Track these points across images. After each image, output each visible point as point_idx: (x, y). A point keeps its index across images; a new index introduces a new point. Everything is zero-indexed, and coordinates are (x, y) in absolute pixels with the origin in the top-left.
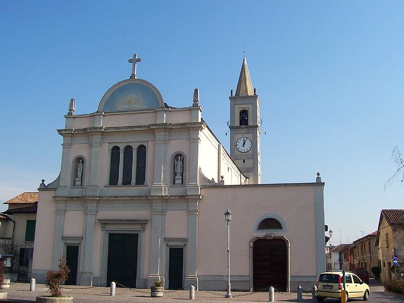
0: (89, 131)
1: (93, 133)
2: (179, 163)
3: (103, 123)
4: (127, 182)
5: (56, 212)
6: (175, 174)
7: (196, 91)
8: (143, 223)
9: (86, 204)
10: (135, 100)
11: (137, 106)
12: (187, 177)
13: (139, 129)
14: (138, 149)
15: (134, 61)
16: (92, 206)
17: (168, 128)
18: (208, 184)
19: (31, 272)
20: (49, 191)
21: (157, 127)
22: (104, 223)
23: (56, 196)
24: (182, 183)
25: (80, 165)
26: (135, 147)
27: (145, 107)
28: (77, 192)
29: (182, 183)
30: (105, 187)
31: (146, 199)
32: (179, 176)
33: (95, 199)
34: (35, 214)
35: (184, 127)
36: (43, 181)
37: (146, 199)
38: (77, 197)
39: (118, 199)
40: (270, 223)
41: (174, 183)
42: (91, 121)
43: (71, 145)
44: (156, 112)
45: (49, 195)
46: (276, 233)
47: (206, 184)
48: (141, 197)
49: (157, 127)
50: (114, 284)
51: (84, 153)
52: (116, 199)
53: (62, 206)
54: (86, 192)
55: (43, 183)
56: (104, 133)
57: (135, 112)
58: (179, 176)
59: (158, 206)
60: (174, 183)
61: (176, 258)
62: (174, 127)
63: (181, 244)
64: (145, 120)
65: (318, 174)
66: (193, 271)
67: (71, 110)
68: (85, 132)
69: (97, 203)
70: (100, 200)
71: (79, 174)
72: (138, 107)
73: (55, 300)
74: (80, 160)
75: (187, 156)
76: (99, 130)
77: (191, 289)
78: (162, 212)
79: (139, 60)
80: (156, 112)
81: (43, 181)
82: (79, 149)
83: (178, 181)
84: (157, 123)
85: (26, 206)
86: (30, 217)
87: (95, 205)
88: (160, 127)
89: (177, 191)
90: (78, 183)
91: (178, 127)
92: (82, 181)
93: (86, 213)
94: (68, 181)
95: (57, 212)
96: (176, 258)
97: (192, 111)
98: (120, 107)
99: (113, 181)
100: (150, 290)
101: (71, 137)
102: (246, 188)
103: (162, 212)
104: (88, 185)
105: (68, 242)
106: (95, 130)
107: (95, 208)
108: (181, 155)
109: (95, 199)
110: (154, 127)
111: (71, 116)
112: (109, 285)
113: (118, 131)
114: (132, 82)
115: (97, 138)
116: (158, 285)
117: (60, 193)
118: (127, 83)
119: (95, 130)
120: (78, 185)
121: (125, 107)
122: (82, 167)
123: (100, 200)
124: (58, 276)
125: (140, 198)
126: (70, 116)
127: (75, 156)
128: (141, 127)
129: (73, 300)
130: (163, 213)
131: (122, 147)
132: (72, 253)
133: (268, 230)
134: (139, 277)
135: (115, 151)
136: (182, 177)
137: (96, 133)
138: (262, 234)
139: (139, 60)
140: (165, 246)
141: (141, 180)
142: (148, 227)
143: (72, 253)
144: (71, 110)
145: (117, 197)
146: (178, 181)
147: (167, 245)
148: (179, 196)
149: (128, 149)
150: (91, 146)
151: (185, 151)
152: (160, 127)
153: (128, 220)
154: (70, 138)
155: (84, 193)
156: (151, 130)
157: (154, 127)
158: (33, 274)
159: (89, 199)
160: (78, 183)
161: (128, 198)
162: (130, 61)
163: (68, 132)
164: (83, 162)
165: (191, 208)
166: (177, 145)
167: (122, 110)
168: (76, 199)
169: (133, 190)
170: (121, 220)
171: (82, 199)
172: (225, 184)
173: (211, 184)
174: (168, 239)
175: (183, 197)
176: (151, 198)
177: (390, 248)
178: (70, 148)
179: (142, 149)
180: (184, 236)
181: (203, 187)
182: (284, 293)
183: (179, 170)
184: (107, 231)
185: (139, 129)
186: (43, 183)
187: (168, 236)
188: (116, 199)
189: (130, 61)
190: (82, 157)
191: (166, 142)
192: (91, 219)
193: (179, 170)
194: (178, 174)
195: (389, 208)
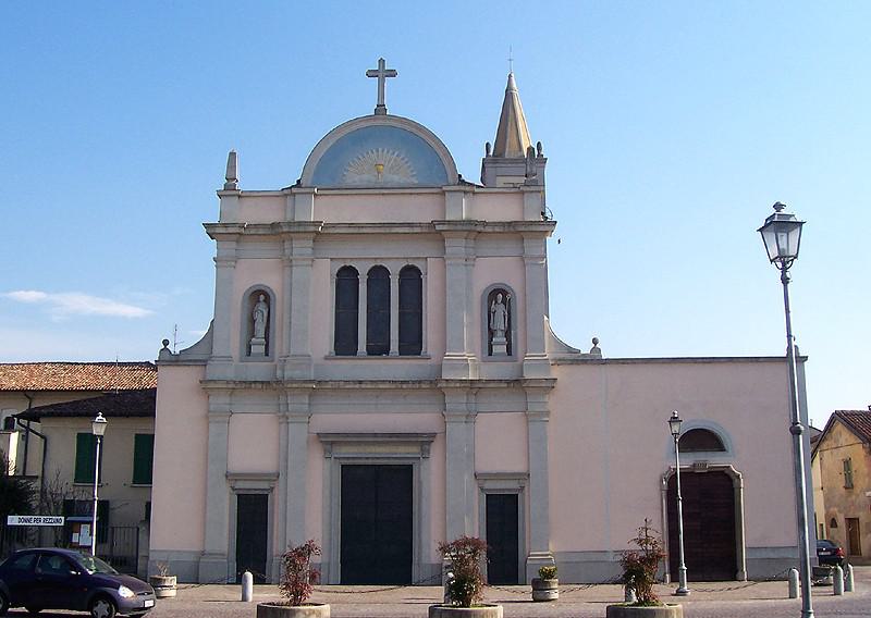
0: (285, 230)
1: (292, 235)
2: (500, 310)
3: (317, 211)
4: (378, 348)
5: (207, 417)
6: (492, 333)
8: (423, 441)
9: (282, 398)
10: (391, 164)
11: (396, 178)
12: (520, 337)
13: (407, 230)
14: (337, 275)
15: (382, 73)
16: (298, 403)
17: (475, 231)
18: (568, 356)
19: (147, 557)
20: (187, 368)
21: (452, 227)
22: (329, 441)
23: (208, 378)
25: (262, 307)
26: (394, 269)
27: (416, 182)
28: (258, 370)
30: (326, 358)
31: (434, 386)
32: (499, 338)
33: (310, 386)
34: (147, 419)
35: (512, 229)
36: (166, 343)
37: (434, 386)
38: (262, 382)
39: (363, 386)
40: (700, 439)
42: (286, 206)
43: (236, 259)
44: (444, 193)
45: (187, 377)
46: (715, 460)
47: (562, 356)
48: (420, 382)
49: (452, 227)
50: (249, 576)
51: (272, 281)
52: (359, 386)
53: (220, 401)
54: (283, 371)
55: (166, 349)
56: (320, 235)
57: (348, 192)
58: (499, 338)
59: (457, 402)
61: (503, 511)
62: (489, 229)
63: (512, 485)
64: (420, 210)
66: (542, 544)
67: (231, 178)
68: (277, 233)
69: (310, 396)
70: (317, 388)
71: (260, 328)
72: (397, 179)
73: (294, 612)
74: (260, 296)
75: (519, 295)
76: (312, 229)
77: (790, 579)
78: (467, 416)
79: (392, 73)
80: (523, 193)
81: (166, 343)
82: (261, 270)
83: (500, 349)
84: (447, 219)
85: (84, 397)
86: (139, 426)
87: (307, 397)
88: (459, 227)
89: (500, 370)
91: (497, 229)
92: (267, 346)
93: (284, 419)
94: (231, 343)
95: (208, 416)
96: (503, 511)
97: (526, 195)
98: (353, 177)
99: (345, 344)
100: (530, 588)
101: (237, 242)
102: (673, 365)
103: (467, 416)
104: (285, 353)
105: (240, 485)
106: (301, 229)
107: (306, 407)
108: (504, 293)
109: (310, 386)
110: (445, 227)
111: (234, 192)
112: (240, 580)
113: (356, 233)
114: (379, 122)
115: (302, 247)
116: (549, 575)
117: (216, 371)
118: (369, 124)
119: (301, 229)
120: (258, 354)
121: (367, 178)
122: (266, 314)
123: (317, 388)
124: (652, 559)
125: (357, 386)
126: (229, 191)
127: (266, 284)
128: (410, 225)
129: (602, 610)
130: (470, 417)
131: (363, 271)
132: (253, 512)
133: (698, 454)
134: (420, 559)
135: (346, 277)
136: (509, 340)
137: (303, 235)
138: (682, 462)
139: (392, 73)
140: (476, 491)
141: (412, 344)
142: (435, 450)
143: (253, 512)
144: (231, 178)
145: (360, 382)
146: (500, 349)
148: (508, 382)
149: (379, 275)
150: (288, 263)
151: (514, 284)
152: (459, 227)
153: (384, 435)
154: (234, 245)
155: (279, 373)
156: (436, 233)
157: (445, 227)
158: (154, 561)
159: (294, 385)
160: (258, 349)
161: (387, 386)
162: (371, 74)
163: (231, 230)
164: (267, 300)
165: (533, 408)
166: (494, 268)
167: (358, 184)
168: (260, 386)
169: (395, 367)
170: (375, 435)
171: (274, 387)
172: (604, 357)
173: (574, 356)
174: (481, 474)
175: (517, 384)
176: (445, 385)
177: (857, 490)
178: (473, 265)
179: (411, 276)
180: (520, 468)
181: (559, 362)
182: (733, 584)
183: (500, 324)
184: (339, 458)
185: (407, 230)
186: (166, 349)
187: (484, 466)
188: (359, 386)
189: (371, 74)
190: (268, 290)
191: (469, 261)
192: (299, 433)
193: (500, 324)
194: (500, 333)
195: (849, 408)
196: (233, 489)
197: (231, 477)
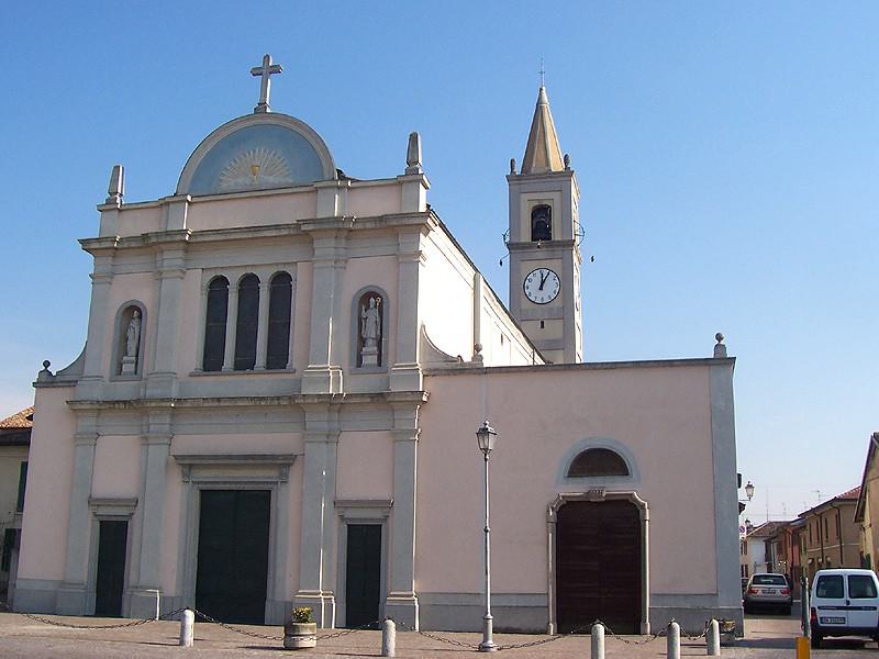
0: (154, 240)
1: (162, 246)
2: (373, 315)
3: (190, 220)
4: (245, 363)
5: (75, 439)
6: (362, 342)
7: (414, 139)
8: (283, 463)
10: (266, 165)
13: (274, 233)
15: (265, 71)
16: (159, 423)
17: (344, 230)
19: (15, 585)
21: (318, 227)
22: (189, 464)
24: (380, 365)
25: (134, 323)
26: (265, 276)
27: (291, 181)
28: (124, 390)
29: (380, 365)
30: (191, 375)
31: (293, 404)
32: (371, 347)
33: (168, 404)
35: (383, 223)
36: (47, 364)
37: (293, 404)
38: (125, 402)
41: (359, 363)
43: (112, 275)
45: (60, 396)
46: (614, 487)
47: (437, 365)
48: (278, 398)
49: (318, 227)
51: (144, 297)
53: (88, 423)
55: (46, 370)
56: (192, 245)
58: (371, 347)
59: (318, 420)
60: (359, 363)
62: (359, 226)
64: (289, 211)
65: (719, 337)
69: (172, 416)
70: (181, 408)
72: (272, 180)
74: (133, 311)
76: (178, 238)
78: (328, 436)
79: (276, 70)
81: (47, 364)
82: (134, 286)
84: (319, 217)
87: (168, 420)
89: (367, 383)
90: (128, 368)
91: (368, 225)
93: (145, 441)
94: (104, 363)
97: (404, 185)
98: (229, 183)
99: (212, 362)
102: (536, 374)
106: (168, 239)
107: (167, 427)
108: (375, 295)
109: (168, 404)
110: (311, 227)
115: (173, 258)
118: (248, 124)
121: (243, 181)
123: (181, 408)
126: (109, 207)
128: (277, 227)
130: (331, 437)
131: (234, 278)
132: (113, 539)
135: (218, 287)
137: (169, 246)
138: (578, 488)
139: (276, 70)
140: (335, 522)
141: (278, 358)
142: (294, 474)
143: (113, 539)
145: (219, 400)
147: (342, 518)
148: (372, 396)
149: (249, 283)
150: (159, 276)
151: (386, 286)
153: (246, 457)
156: (303, 234)
157: (311, 227)
159: (153, 405)
161: (246, 403)
164: (140, 317)
165: (401, 425)
166: (366, 270)
168: (122, 406)
169: (260, 383)
170: (230, 457)
173: (450, 365)
175: (380, 398)
176: (302, 401)
179: (282, 283)
180: (381, 492)
182: (636, 638)
185: (274, 233)
186: (46, 370)
187: (347, 492)
191: (340, 263)
192: (159, 454)
194: (370, 342)
196: (96, 515)
197: (93, 502)
